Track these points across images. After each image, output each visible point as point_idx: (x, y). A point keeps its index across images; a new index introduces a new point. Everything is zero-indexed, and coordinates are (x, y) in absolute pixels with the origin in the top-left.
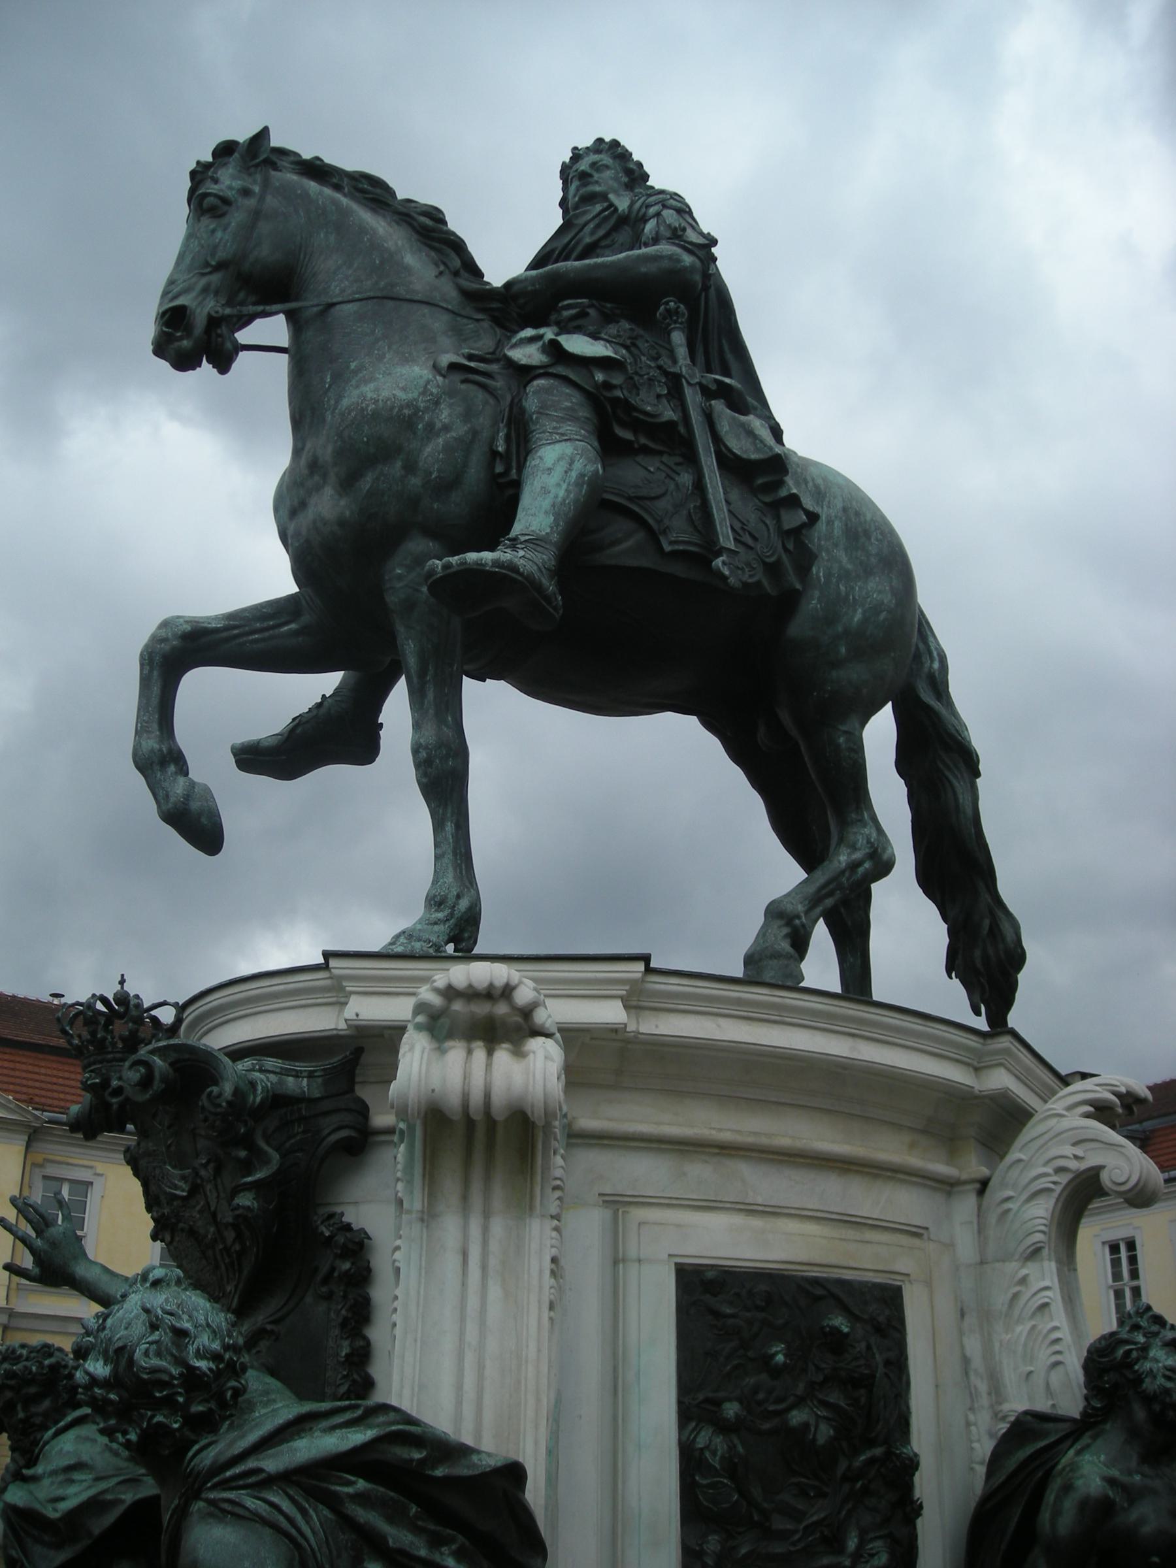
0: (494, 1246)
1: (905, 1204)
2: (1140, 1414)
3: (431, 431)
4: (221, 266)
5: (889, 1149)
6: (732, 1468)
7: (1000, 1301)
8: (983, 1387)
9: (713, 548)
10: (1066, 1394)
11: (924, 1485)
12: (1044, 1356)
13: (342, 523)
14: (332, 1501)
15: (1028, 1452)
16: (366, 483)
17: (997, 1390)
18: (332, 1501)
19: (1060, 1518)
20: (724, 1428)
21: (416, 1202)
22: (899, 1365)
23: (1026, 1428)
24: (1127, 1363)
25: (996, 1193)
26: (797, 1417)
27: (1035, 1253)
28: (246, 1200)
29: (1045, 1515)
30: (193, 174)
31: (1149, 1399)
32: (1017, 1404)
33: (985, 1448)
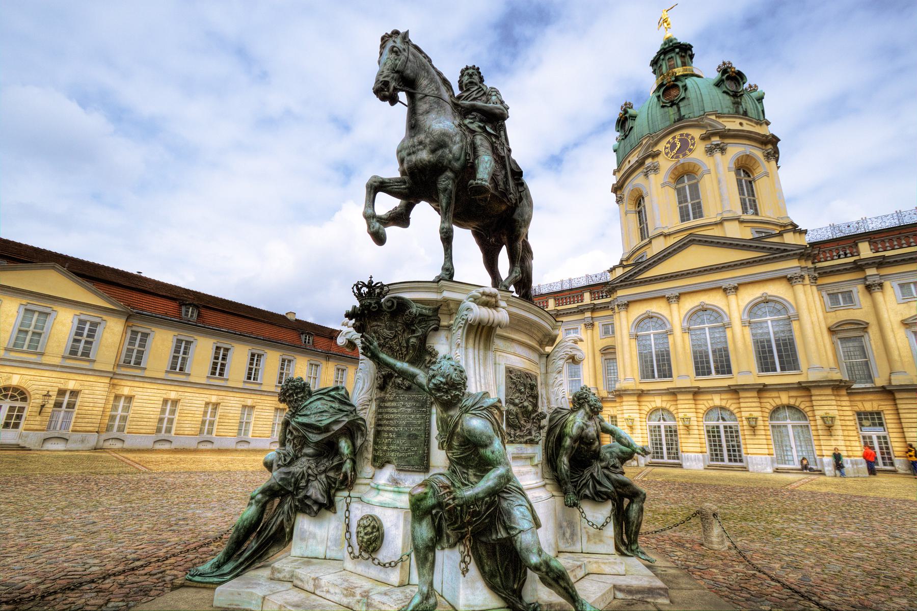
0: (481, 357)
2: (588, 410)
7: (551, 382)
8: (545, 401)
12: (561, 395)
13: (429, 162)
16: (440, 152)
17: (549, 402)
20: (515, 405)
21: (463, 345)
25: (551, 358)
26: (526, 404)
30: (383, 39)
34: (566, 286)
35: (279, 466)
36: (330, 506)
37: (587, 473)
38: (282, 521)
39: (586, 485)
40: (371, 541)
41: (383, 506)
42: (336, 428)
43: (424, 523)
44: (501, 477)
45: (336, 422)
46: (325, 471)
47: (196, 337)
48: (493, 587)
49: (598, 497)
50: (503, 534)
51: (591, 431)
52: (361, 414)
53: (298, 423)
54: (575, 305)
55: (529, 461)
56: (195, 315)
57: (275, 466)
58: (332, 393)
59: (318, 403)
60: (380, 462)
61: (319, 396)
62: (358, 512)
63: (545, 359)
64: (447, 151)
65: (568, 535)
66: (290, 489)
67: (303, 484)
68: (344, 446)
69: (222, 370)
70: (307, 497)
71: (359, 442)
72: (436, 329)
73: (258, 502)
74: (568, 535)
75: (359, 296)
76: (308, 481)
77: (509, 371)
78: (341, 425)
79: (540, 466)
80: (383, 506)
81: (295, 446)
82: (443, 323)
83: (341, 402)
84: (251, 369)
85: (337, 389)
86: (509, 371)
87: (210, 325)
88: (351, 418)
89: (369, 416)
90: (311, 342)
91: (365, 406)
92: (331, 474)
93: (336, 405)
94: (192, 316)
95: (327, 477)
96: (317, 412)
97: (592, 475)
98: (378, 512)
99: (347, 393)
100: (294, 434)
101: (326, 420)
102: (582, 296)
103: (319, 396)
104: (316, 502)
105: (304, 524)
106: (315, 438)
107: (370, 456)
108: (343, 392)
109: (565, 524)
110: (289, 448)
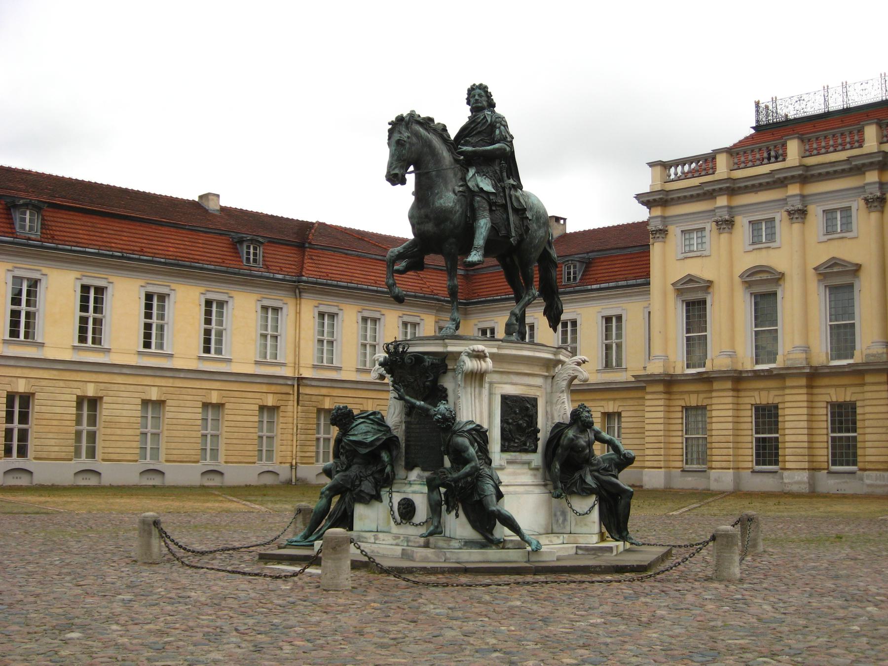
1: (539, 381)
2: (580, 423)
3: (456, 213)
4: (404, 160)
5: (536, 371)
6: (510, 431)
7: (555, 401)
9: (508, 236)
10: (567, 420)
11: (539, 435)
12: (563, 412)
14: (471, 434)
15: (558, 430)
17: (553, 418)
18: (471, 434)
19: (564, 441)
20: (508, 424)
22: (537, 413)
23: (558, 425)
24: (579, 414)
25: (556, 379)
26: (521, 422)
27: (563, 392)
28: (428, 383)
29: (561, 441)
31: (582, 421)
32: (557, 421)
33: (550, 429)
34: (836, 104)
35: (338, 472)
36: (378, 498)
37: (577, 475)
38: (345, 509)
39: (575, 484)
40: (407, 510)
41: (414, 492)
42: (378, 443)
43: (435, 493)
44: (472, 467)
45: (378, 439)
46: (372, 475)
47: (45, 270)
48: (474, 527)
49: (586, 491)
50: (477, 498)
51: (582, 442)
52: (395, 433)
53: (350, 441)
54: (842, 156)
55: (526, 466)
56: (37, 225)
57: (334, 472)
58: (371, 417)
59: (362, 426)
60: (410, 467)
61: (362, 420)
62: (397, 498)
63: (550, 380)
64: (448, 223)
65: (560, 521)
66: (349, 486)
67: (357, 483)
68: (385, 456)
69: (97, 331)
70: (361, 491)
71: (395, 453)
72: (445, 373)
73: (327, 496)
74: (560, 521)
75: (388, 352)
76: (361, 481)
77: (505, 398)
78: (381, 442)
79: (541, 470)
80: (414, 492)
81: (347, 457)
82: (449, 367)
83: (379, 424)
84: (148, 327)
85: (374, 413)
86: (505, 398)
87: (65, 242)
88: (388, 435)
89: (399, 433)
90: (260, 258)
91: (397, 426)
92: (377, 476)
93: (375, 427)
94: (31, 228)
95: (374, 478)
96: (362, 432)
97: (581, 476)
98: (410, 496)
99: (383, 417)
100: (345, 450)
101: (370, 438)
102: (861, 131)
103: (362, 420)
104: (368, 494)
105: (360, 510)
106: (364, 451)
107: (403, 463)
108: (379, 416)
109: (559, 513)
110: (343, 458)
